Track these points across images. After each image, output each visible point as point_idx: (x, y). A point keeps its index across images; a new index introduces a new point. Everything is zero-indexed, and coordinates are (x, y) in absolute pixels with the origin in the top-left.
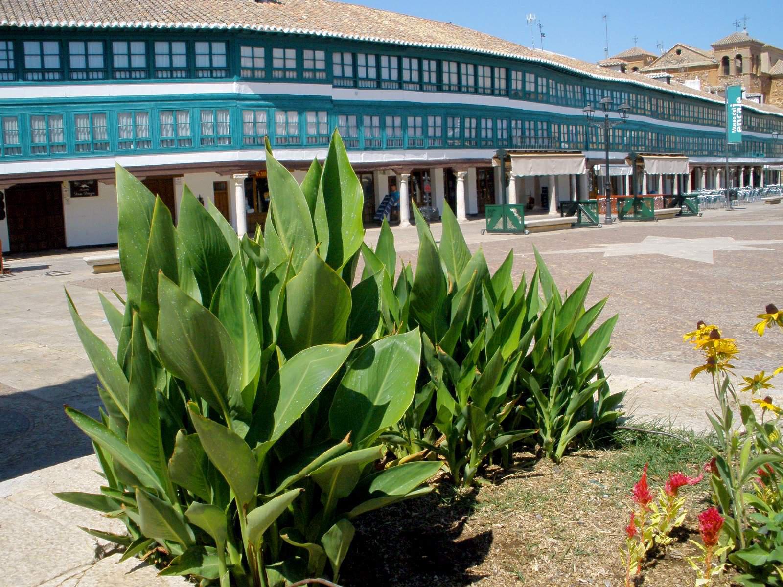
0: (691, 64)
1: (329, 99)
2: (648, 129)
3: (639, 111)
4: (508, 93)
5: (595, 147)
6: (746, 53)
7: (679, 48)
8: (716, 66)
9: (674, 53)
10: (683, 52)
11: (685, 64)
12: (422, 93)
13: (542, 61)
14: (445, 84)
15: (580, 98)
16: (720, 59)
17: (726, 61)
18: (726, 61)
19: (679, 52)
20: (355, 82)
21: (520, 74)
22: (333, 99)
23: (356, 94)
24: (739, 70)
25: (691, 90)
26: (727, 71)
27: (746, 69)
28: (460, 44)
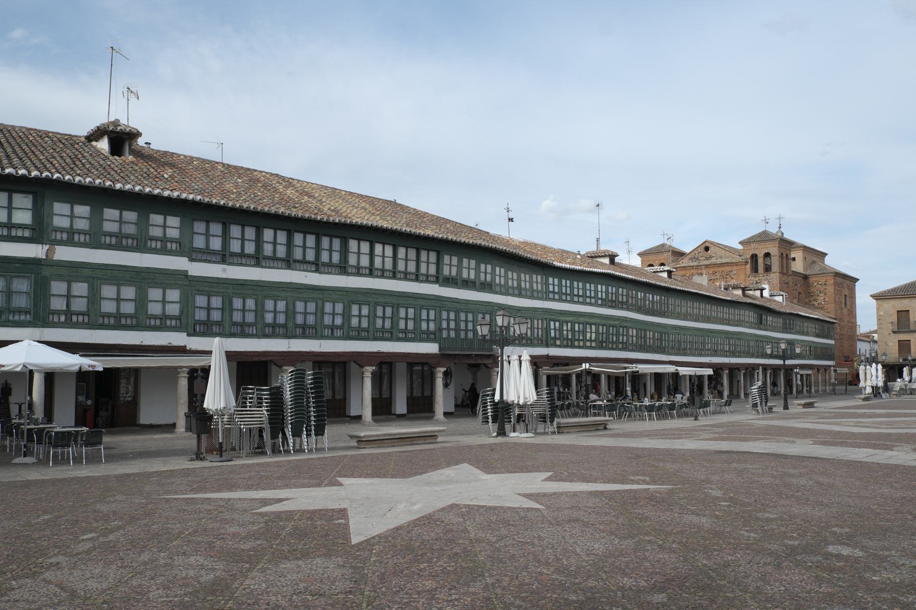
0: (719, 261)
1: (184, 274)
2: (628, 325)
3: (576, 299)
4: (441, 279)
5: (581, 344)
6: (774, 250)
7: (707, 244)
8: (746, 263)
9: (702, 250)
10: (712, 249)
11: (713, 261)
12: (317, 275)
13: (483, 244)
14: (352, 266)
15: (539, 288)
16: (749, 256)
17: (754, 257)
18: (754, 257)
19: (707, 249)
20: (224, 257)
21: (455, 260)
22: (190, 274)
23: (224, 270)
24: (768, 269)
25: (700, 286)
26: (755, 269)
27: (775, 267)
28: (183, 192)
